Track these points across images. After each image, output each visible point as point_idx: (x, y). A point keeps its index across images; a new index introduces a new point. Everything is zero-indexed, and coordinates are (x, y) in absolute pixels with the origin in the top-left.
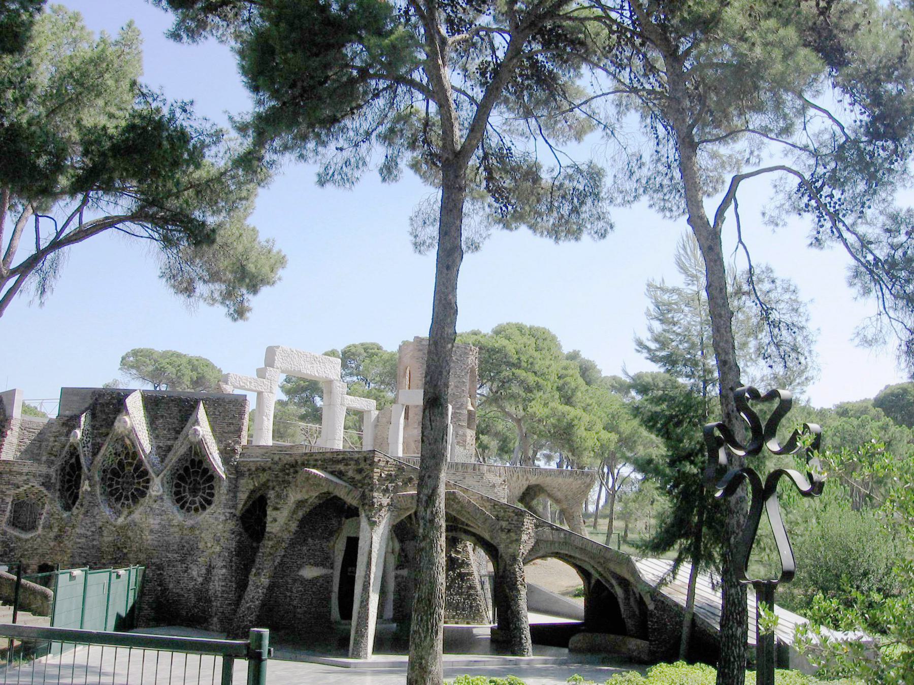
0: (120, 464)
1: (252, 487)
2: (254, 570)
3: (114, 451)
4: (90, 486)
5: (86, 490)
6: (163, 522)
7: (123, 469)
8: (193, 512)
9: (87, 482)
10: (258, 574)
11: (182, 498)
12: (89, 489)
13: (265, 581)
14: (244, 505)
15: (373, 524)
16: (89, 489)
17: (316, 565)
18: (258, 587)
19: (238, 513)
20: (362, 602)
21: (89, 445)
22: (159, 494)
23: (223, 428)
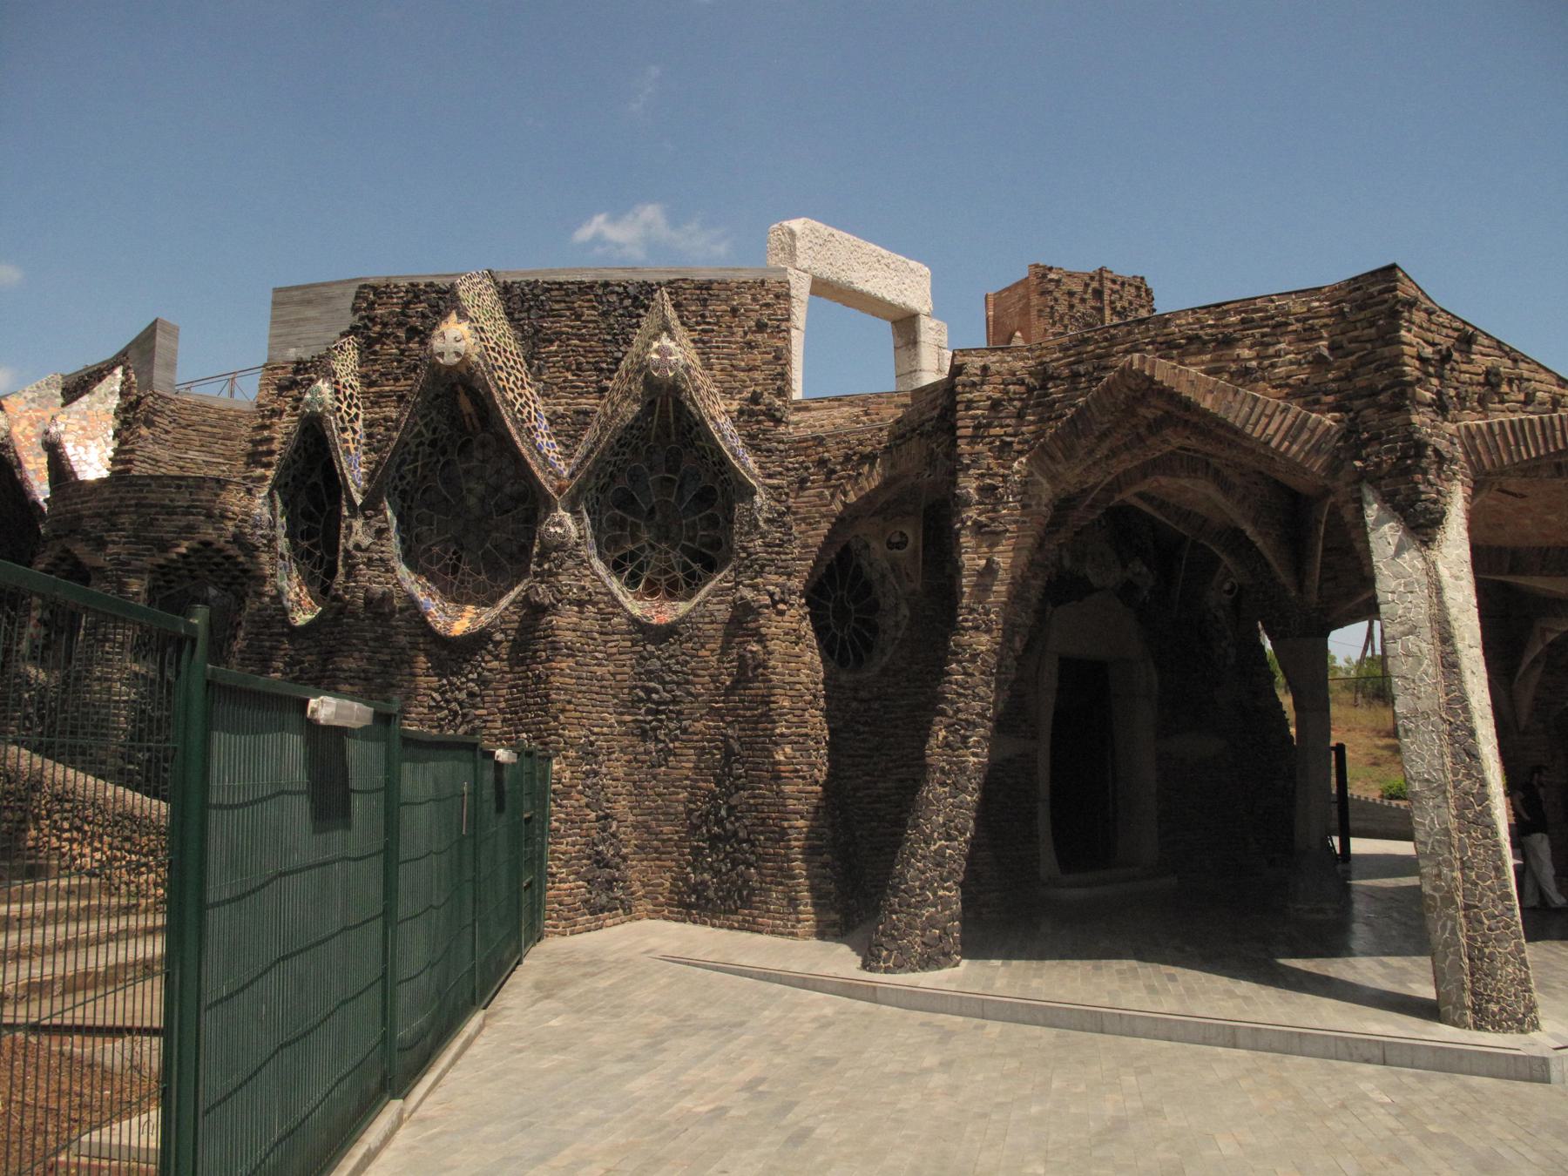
1: (837, 507)
3: (428, 436)
6: (586, 625)
9: (358, 524)
15: (1422, 526)
19: (796, 583)
20: (1462, 807)
21: (359, 425)
23: (730, 356)
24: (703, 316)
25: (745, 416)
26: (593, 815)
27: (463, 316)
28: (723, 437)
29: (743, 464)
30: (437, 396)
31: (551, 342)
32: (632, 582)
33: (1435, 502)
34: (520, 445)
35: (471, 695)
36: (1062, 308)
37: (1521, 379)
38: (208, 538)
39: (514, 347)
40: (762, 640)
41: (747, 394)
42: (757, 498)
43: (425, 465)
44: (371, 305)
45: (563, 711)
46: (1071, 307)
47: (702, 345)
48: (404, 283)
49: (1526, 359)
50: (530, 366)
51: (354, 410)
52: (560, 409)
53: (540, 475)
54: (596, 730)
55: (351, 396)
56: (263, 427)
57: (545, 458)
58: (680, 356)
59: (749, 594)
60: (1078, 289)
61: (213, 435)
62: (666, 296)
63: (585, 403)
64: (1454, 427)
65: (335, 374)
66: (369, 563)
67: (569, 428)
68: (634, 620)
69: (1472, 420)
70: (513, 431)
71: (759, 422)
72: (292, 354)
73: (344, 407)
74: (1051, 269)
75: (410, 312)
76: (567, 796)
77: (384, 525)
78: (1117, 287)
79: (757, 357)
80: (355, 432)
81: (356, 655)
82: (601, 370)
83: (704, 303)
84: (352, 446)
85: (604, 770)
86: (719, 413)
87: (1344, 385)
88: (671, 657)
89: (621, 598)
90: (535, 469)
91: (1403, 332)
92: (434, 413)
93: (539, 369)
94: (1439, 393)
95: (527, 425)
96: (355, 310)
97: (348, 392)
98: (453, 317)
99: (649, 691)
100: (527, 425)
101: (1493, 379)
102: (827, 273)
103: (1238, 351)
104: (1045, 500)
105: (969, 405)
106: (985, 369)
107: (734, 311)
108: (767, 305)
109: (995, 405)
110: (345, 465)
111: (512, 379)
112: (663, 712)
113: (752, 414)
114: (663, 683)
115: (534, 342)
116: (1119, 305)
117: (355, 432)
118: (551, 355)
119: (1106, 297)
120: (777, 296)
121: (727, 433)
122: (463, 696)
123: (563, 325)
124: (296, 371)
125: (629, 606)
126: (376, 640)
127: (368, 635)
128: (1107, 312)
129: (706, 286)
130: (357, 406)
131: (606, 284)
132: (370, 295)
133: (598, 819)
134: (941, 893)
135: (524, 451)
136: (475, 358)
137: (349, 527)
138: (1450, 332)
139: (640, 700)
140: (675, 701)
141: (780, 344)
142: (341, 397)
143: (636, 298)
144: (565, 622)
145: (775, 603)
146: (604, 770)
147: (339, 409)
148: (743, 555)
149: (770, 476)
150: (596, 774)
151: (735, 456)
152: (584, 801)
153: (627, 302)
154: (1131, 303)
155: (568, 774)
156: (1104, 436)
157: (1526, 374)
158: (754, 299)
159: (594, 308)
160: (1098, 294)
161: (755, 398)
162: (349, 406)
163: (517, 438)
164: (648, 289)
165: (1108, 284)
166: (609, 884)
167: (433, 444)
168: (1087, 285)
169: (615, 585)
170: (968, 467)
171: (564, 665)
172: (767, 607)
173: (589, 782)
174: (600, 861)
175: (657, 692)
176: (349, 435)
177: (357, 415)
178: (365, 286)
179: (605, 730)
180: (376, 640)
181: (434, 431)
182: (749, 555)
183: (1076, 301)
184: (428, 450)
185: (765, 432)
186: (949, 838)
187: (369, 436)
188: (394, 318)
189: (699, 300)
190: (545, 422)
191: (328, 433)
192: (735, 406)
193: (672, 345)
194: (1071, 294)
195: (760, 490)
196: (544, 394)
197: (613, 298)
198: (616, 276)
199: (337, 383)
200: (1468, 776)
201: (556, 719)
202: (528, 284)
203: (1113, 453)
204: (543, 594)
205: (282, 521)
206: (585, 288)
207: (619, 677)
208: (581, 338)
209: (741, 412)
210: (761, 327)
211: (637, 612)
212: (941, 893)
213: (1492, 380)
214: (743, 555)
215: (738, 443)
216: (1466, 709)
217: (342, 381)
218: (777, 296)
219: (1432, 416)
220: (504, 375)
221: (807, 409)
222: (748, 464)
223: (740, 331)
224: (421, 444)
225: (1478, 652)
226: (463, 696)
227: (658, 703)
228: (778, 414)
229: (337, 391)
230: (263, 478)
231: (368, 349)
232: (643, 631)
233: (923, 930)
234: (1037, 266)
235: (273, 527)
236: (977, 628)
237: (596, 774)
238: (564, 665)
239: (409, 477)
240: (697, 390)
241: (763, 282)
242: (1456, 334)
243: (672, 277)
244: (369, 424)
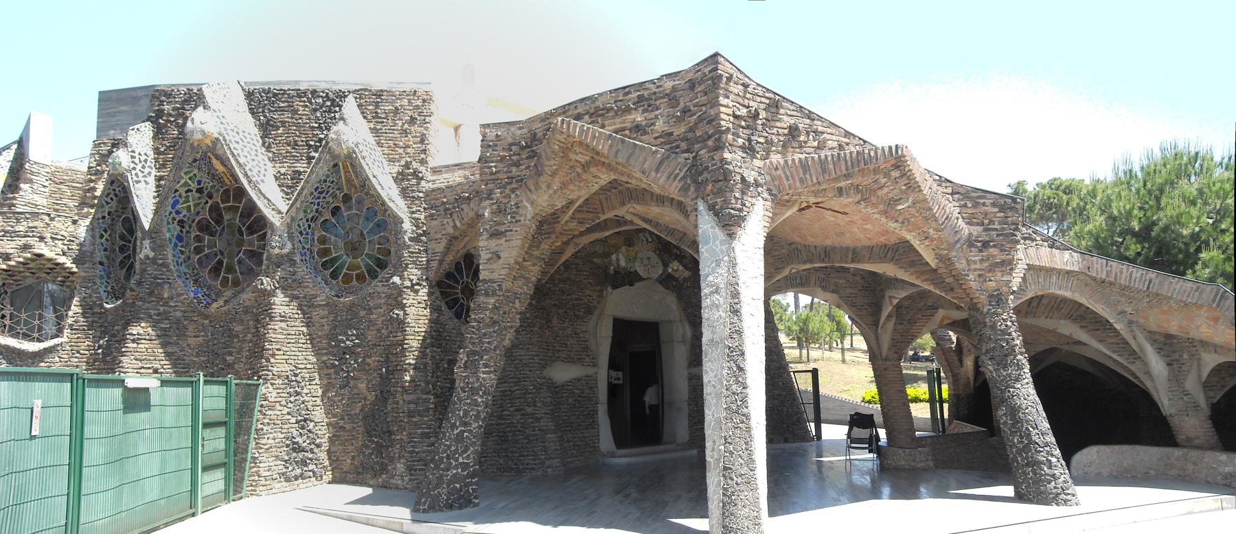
0: (215, 209)
2: (462, 357)
3: (194, 186)
4: (153, 249)
5: (147, 257)
7: (219, 221)
8: (355, 282)
9: (147, 243)
10: (471, 366)
11: (335, 260)
12: (152, 255)
13: (487, 377)
14: (441, 262)
15: (730, 223)
16: (152, 255)
17: (570, 360)
18: (474, 391)
21: (151, 180)
22: (286, 251)
26: (293, 420)
30: (195, 161)
33: (740, 210)
40: (403, 307)
43: (196, 205)
45: (273, 355)
49: (820, 118)
50: (264, 143)
52: (283, 170)
55: (146, 161)
56: (91, 181)
63: (301, 166)
67: (288, 183)
76: (272, 408)
82: (310, 146)
83: (377, 105)
85: (305, 391)
87: (690, 135)
92: (196, 171)
97: (143, 158)
103: (632, 117)
104: (529, 216)
115: (266, 128)
118: (277, 136)
120: (424, 101)
126: (158, 315)
127: (152, 312)
129: (379, 94)
132: (158, 95)
133: (297, 422)
134: (461, 460)
138: (763, 100)
142: (137, 160)
145: (413, 285)
146: (305, 391)
150: (298, 394)
152: (286, 410)
153: (329, 103)
155: (274, 394)
156: (554, 174)
157: (820, 129)
164: (342, 95)
166: (304, 463)
167: (200, 191)
173: (292, 399)
174: (297, 449)
180: (158, 315)
181: (199, 182)
184: (198, 195)
186: (465, 424)
187: (157, 186)
189: (375, 103)
197: (320, 100)
198: (321, 86)
201: (268, 360)
206: (301, 94)
213: (793, 131)
218: (424, 101)
223: (400, 123)
224: (189, 191)
229: (133, 157)
230: (89, 214)
231: (159, 133)
236: (487, 295)
237: (298, 394)
239: (185, 212)
243: (358, 88)
244: (159, 179)
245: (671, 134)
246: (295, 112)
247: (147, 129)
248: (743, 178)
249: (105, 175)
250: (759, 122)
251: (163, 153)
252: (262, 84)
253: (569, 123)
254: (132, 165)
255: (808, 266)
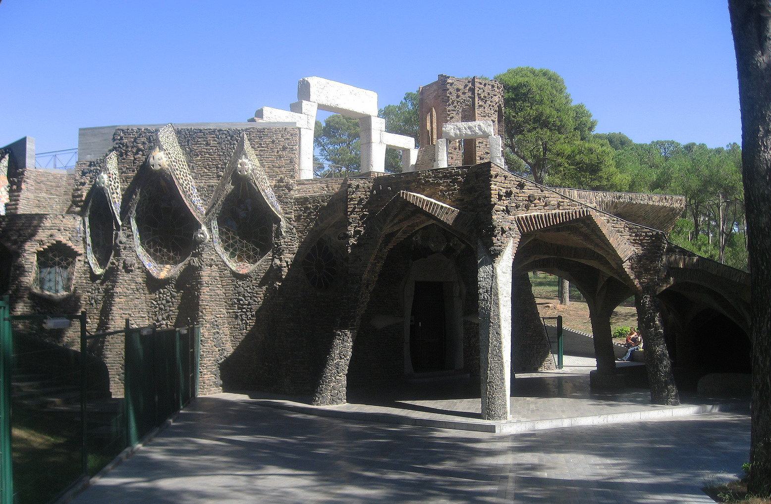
6: (213, 274)
24: (261, 144)
25: (276, 188)
26: (217, 349)
27: (161, 149)
28: (268, 199)
29: (276, 209)
31: (198, 155)
32: (232, 255)
33: (500, 246)
34: (186, 202)
35: (168, 302)
36: (453, 97)
37: (545, 197)
38: (59, 239)
39: (183, 158)
41: (278, 178)
42: (281, 223)
44: (121, 138)
46: (458, 96)
47: (260, 157)
48: (135, 129)
50: (189, 166)
51: (117, 184)
52: (202, 185)
53: (194, 213)
54: (218, 316)
57: (196, 206)
58: (250, 166)
59: (277, 262)
60: (461, 87)
61: (51, 186)
62: (245, 136)
64: (513, 217)
65: (108, 169)
66: (125, 248)
68: (232, 272)
69: (522, 214)
70: (183, 196)
71: (283, 190)
72: (89, 158)
73: (113, 183)
74: (448, 77)
75: (139, 141)
77: (131, 233)
78: (482, 86)
79: (283, 161)
80: (117, 193)
81: (122, 286)
82: (217, 168)
84: (116, 200)
86: (267, 189)
88: (248, 287)
89: (228, 263)
90: (192, 211)
91: (492, 186)
93: (193, 167)
94: (507, 207)
95: (189, 193)
96: (114, 139)
98: (158, 149)
99: (239, 300)
100: (189, 193)
101: (531, 199)
102: (324, 101)
105: (352, 199)
106: (358, 185)
107: (273, 142)
108: (288, 139)
109: (361, 200)
110: (114, 208)
111: (182, 173)
112: (244, 308)
113: (279, 187)
114: (244, 296)
115: (190, 155)
116: (482, 96)
117: (117, 193)
119: (476, 92)
121: (269, 196)
122: (164, 302)
123: (204, 148)
124: (90, 165)
125: (231, 266)
128: (477, 99)
130: (118, 182)
131: (220, 130)
133: (219, 350)
134: (338, 378)
135: (187, 204)
136: (167, 166)
137: (117, 235)
138: (515, 183)
139: (236, 304)
140: (249, 304)
141: (293, 156)
142: (111, 180)
143: (232, 137)
144: (206, 274)
146: (221, 332)
147: (111, 185)
148: (276, 246)
149: (286, 213)
150: (218, 333)
151: (273, 206)
154: (489, 94)
156: (396, 216)
158: (282, 137)
159: (215, 140)
160: (472, 90)
161: (281, 180)
162: (115, 183)
163: (184, 199)
165: (477, 85)
168: (466, 86)
169: (226, 257)
170: (351, 223)
171: (205, 291)
172: (285, 267)
175: (242, 300)
176: (115, 195)
177: (118, 187)
178: (119, 130)
179: (222, 316)
182: (278, 246)
183: (460, 93)
185: (285, 194)
188: (133, 144)
190: (196, 190)
191: (107, 195)
192: (274, 182)
193: (246, 161)
194: (458, 90)
195: (282, 219)
196: (195, 178)
199: (109, 173)
200: (496, 340)
201: (202, 312)
202: (188, 130)
203: (400, 221)
204: (196, 261)
205: (88, 230)
207: (227, 295)
208: (210, 154)
209: (275, 186)
210: (284, 148)
211: (234, 269)
212: (338, 378)
214: (276, 246)
215: (274, 200)
216: (498, 318)
217: (111, 172)
219: (503, 214)
220: (178, 172)
221: (303, 184)
222: (277, 209)
223: (276, 150)
225: (509, 299)
226: (164, 302)
227: (243, 305)
228: (291, 187)
229: (110, 177)
232: (236, 276)
233: (331, 390)
234: (442, 75)
235: (85, 232)
238: (205, 291)
240: (257, 179)
241: (286, 129)
242: (518, 183)
245: (463, 200)
246: (207, 144)
247: (113, 156)
248: (502, 228)
249: (87, 185)
250: (513, 195)
251: (124, 172)
252: (188, 125)
253: (407, 194)
254: (110, 182)
255: (547, 257)
